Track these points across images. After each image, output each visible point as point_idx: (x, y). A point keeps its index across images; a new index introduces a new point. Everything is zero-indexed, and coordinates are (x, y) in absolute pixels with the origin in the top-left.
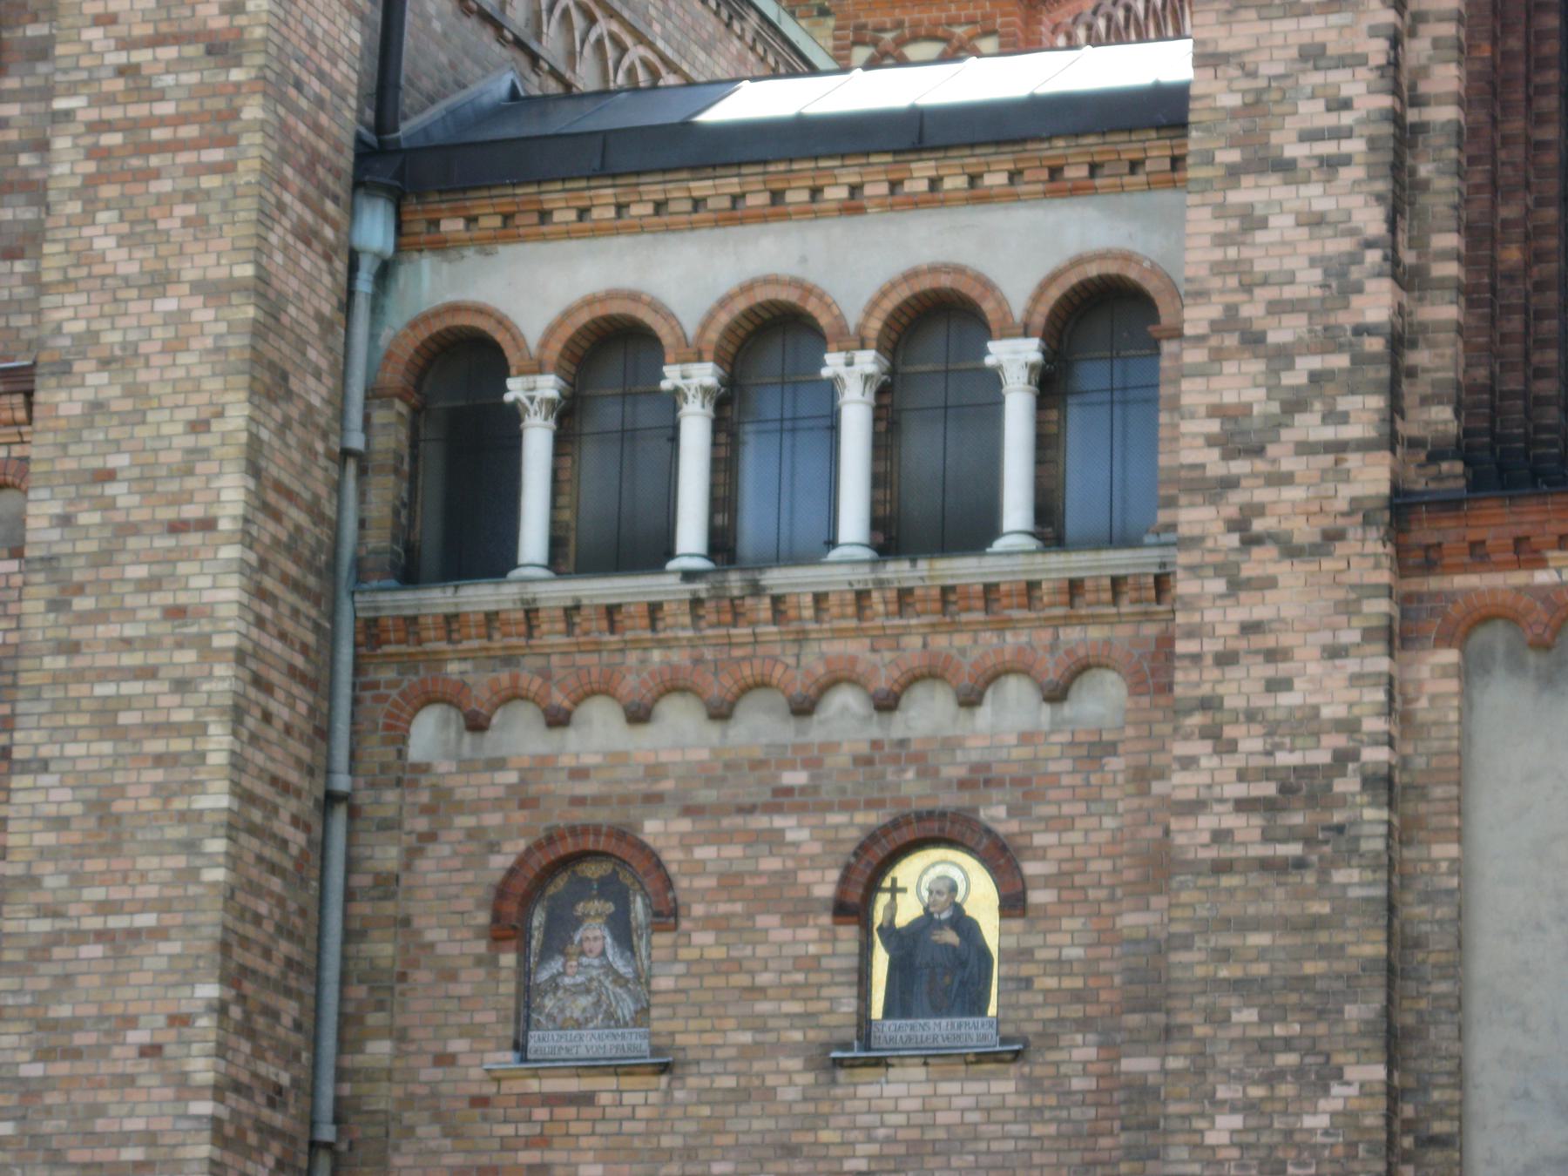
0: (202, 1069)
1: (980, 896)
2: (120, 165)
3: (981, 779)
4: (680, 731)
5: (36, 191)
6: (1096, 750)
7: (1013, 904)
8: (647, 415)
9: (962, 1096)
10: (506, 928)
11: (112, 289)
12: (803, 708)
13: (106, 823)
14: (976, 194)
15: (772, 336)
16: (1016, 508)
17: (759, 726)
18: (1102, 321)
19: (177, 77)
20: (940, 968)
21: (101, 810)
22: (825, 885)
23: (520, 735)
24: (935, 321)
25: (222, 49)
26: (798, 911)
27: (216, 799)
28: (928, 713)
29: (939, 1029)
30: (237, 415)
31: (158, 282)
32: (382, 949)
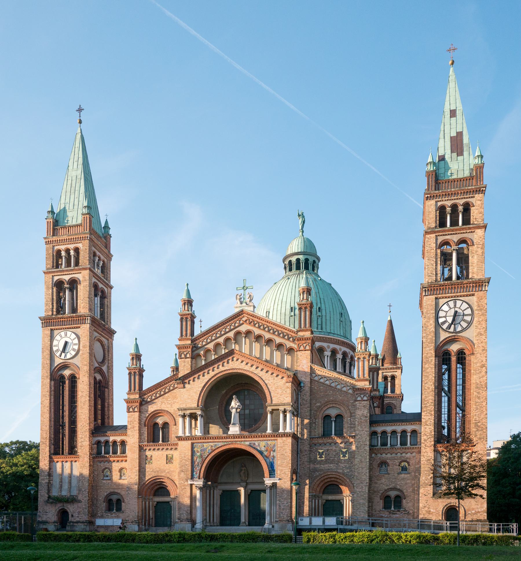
0: (368, 475)
1: (406, 464)
2: (360, 423)
3: (407, 458)
4: (389, 455)
5: (355, 424)
6: (414, 457)
7: (409, 465)
8: (385, 437)
9: (406, 476)
10: (379, 466)
11: (360, 431)
12: (396, 454)
13: (361, 461)
14: (407, 425)
15: (394, 432)
16: (409, 443)
17: (394, 455)
18: (414, 432)
19: (363, 418)
20: (404, 469)
21: (361, 461)
22: (398, 464)
23: (379, 455)
24: (404, 432)
25: (366, 417)
26: (396, 465)
27: (368, 460)
28: (404, 455)
29: (404, 472)
30: (368, 439)
31: (363, 430)
32: (371, 467)
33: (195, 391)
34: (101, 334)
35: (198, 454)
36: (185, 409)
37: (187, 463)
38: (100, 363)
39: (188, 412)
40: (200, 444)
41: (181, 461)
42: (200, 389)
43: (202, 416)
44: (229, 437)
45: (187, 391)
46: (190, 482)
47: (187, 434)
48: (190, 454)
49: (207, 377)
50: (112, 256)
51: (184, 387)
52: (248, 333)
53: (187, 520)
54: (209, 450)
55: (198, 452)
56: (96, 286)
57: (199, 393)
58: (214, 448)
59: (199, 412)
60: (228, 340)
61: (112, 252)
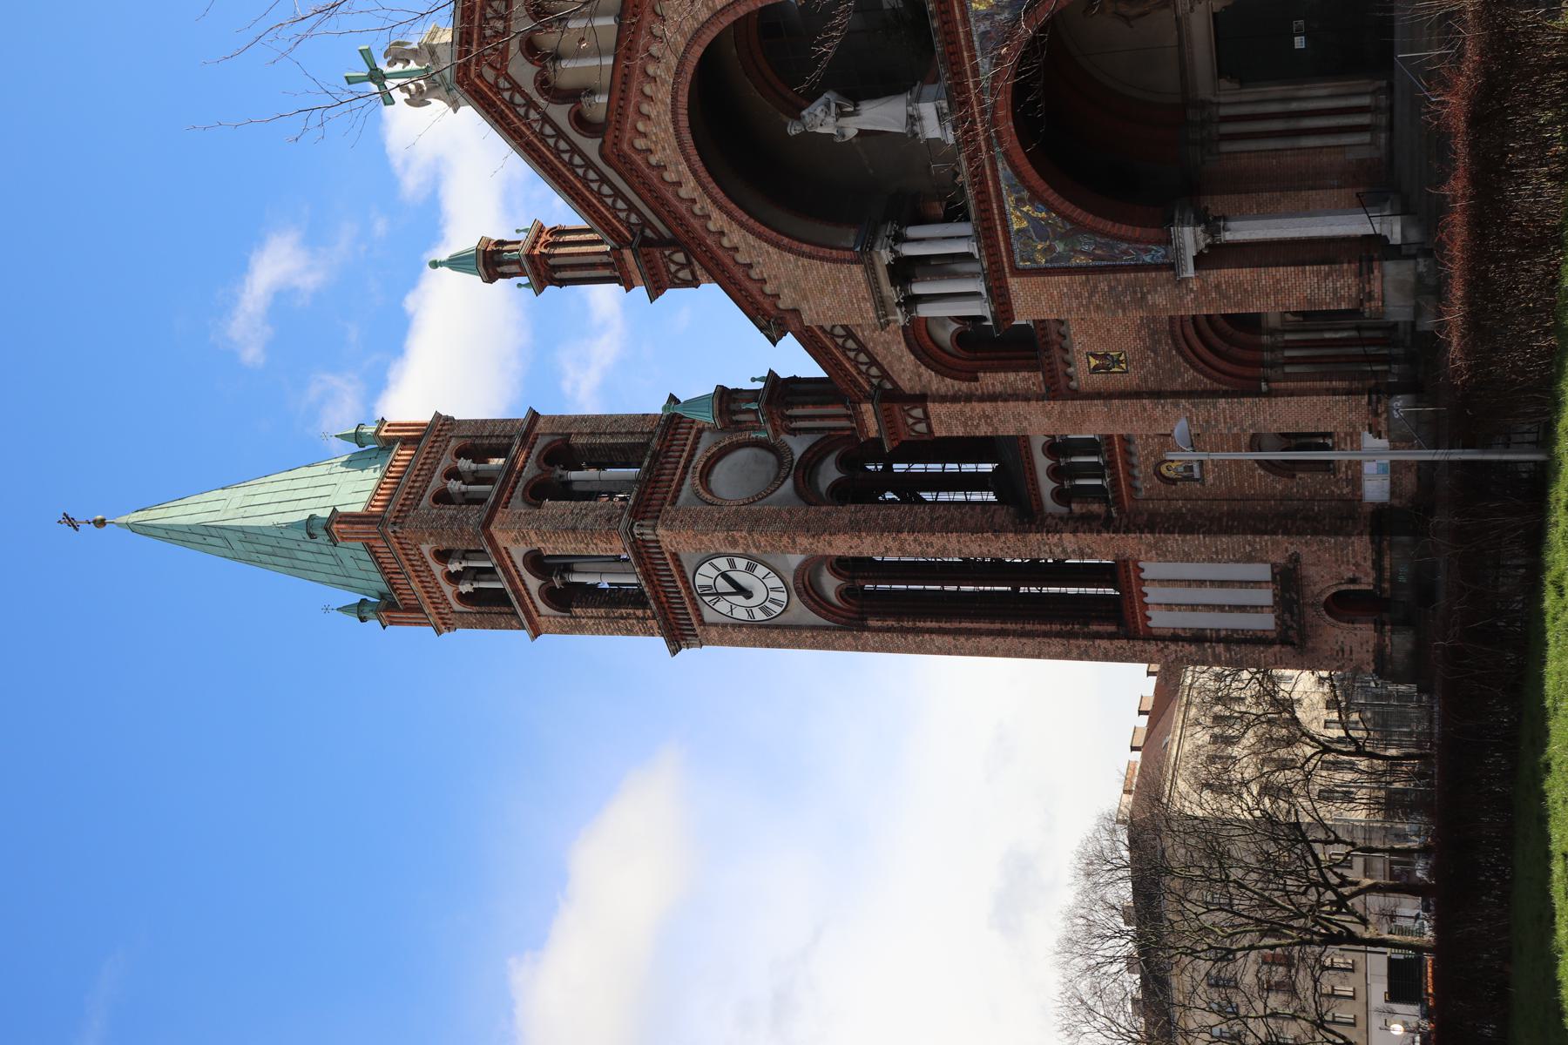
33: (799, 272)
34: (686, 468)
35: (1060, 247)
36: (881, 303)
37: (1103, 286)
38: (780, 464)
39: (890, 293)
40: (1017, 246)
41: (1098, 307)
42: (792, 257)
43: (900, 239)
44: (967, 139)
45: (805, 298)
46: (1190, 272)
47: (978, 286)
48: (1066, 278)
49: (735, 236)
50: (438, 416)
51: (796, 312)
52: (531, 48)
53: (1364, 274)
54: (1037, 209)
55: (1050, 249)
56: (538, 493)
57: (806, 261)
58: (1025, 194)
59: (885, 256)
60: (581, 122)
61: (427, 418)
